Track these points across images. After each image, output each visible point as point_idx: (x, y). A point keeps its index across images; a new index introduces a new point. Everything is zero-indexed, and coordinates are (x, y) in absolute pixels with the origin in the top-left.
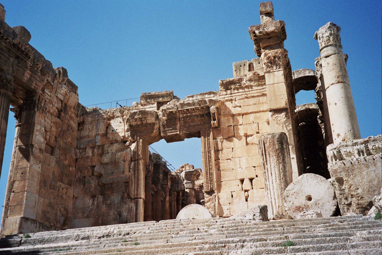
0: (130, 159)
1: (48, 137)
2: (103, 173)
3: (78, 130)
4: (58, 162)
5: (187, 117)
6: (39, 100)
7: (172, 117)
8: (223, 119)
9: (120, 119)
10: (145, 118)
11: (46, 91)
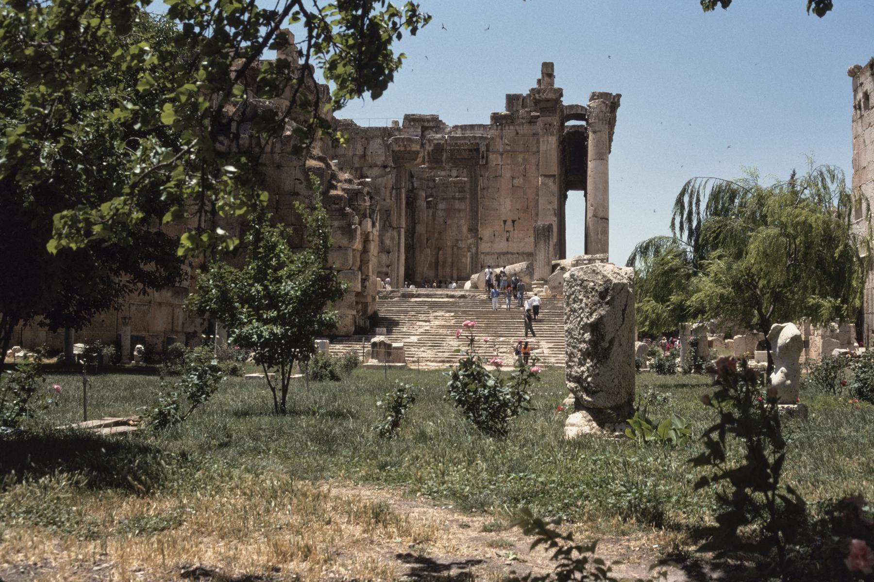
7: (439, 148)
8: (492, 156)
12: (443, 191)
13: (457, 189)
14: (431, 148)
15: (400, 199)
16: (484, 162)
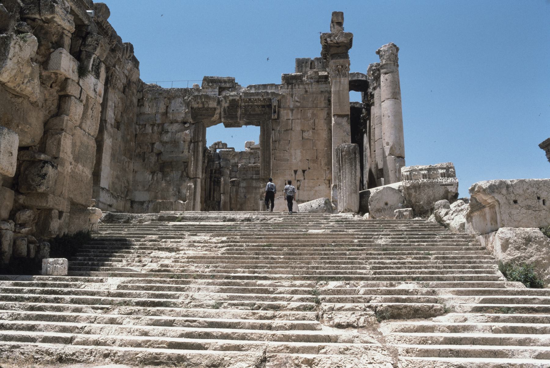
0: (189, 140)
1: (116, 113)
2: (162, 150)
3: (138, 106)
4: (123, 137)
5: (249, 105)
6: (111, 76)
7: (234, 105)
8: (283, 112)
9: (180, 100)
10: (207, 102)
11: (117, 67)
12: (244, 174)
13: (254, 172)
14: (227, 105)
15: (198, 151)
16: (276, 117)
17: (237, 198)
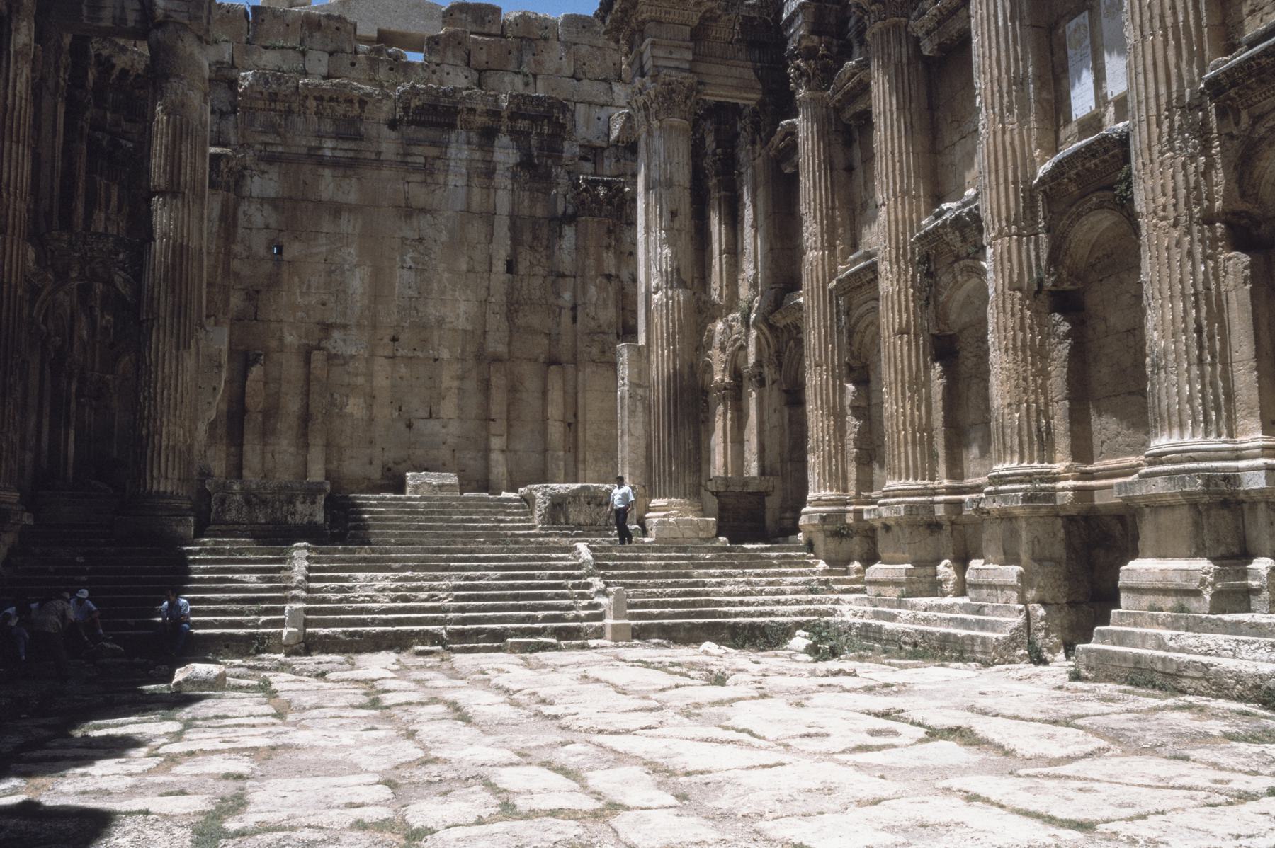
12: (271, 128)
13: (328, 126)
17: (229, 254)
